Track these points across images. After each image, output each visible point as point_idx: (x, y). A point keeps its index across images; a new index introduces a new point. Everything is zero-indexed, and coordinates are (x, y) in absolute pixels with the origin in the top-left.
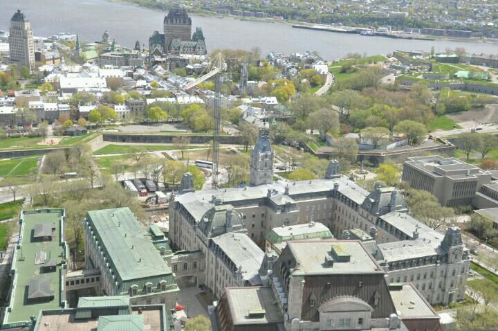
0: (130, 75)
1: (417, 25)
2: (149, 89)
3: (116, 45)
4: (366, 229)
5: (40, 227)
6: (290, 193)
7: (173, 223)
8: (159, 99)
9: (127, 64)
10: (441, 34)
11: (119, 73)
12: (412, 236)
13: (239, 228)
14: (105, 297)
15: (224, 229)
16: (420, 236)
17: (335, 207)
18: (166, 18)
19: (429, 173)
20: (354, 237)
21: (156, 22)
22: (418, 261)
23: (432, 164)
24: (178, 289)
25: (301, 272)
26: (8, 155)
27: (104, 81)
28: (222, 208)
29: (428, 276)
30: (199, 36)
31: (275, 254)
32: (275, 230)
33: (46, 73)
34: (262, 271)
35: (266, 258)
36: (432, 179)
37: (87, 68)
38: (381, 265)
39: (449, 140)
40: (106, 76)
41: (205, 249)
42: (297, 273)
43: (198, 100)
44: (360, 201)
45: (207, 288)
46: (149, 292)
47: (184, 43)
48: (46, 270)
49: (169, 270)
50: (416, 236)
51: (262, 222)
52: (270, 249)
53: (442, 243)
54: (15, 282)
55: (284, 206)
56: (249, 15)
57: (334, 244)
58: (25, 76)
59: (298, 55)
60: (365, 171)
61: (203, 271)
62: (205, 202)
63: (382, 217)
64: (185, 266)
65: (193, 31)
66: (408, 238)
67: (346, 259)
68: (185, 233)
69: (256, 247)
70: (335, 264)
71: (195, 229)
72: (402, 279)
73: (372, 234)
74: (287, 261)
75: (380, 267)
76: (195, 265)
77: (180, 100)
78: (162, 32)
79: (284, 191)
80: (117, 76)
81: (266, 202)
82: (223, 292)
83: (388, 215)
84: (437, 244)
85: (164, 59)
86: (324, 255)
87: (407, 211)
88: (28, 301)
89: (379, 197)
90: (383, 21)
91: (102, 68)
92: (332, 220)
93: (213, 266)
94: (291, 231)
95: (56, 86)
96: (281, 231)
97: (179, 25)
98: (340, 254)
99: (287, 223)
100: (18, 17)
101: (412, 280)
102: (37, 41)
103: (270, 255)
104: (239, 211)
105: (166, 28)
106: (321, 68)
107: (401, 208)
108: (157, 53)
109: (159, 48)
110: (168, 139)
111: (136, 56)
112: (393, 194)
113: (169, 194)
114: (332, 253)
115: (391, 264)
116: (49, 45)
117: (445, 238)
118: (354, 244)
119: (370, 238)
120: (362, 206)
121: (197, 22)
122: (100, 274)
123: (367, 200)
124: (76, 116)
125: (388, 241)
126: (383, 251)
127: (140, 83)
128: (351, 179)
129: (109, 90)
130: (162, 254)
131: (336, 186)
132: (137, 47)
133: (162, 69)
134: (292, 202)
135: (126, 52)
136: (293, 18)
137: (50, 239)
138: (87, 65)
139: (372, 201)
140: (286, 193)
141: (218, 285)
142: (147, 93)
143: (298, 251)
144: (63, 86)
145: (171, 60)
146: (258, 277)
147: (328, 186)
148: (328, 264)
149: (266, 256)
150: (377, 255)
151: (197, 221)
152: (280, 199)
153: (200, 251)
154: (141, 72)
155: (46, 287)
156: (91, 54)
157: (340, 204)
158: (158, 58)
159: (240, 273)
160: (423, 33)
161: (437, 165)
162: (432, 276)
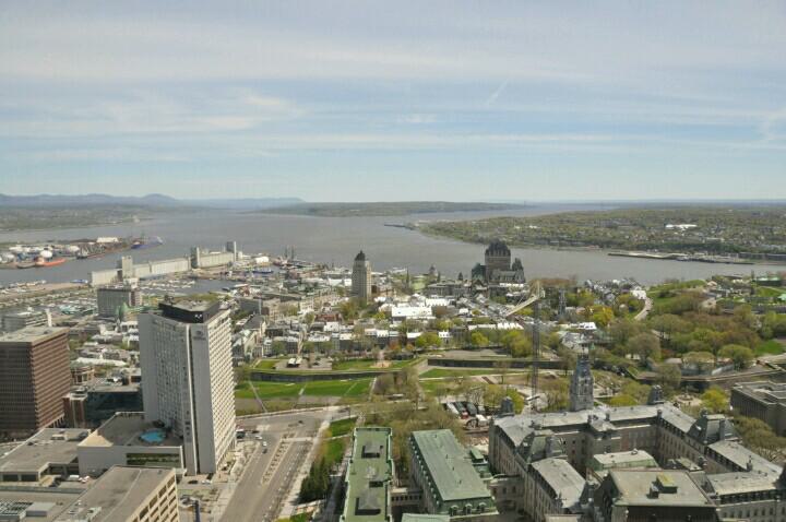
0: (454, 303)
1: (734, 251)
2: (471, 316)
3: (442, 277)
4: (693, 459)
5: (370, 444)
6: (612, 419)
8: (481, 326)
9: (451, 294)
10: (760, 257)
11: (443, 302)
12: (745, 467)
13: (559, 454)
14: (427, 515)
15: (543, 455)
16: (754, 468)
17: (658, 435)
18: (487, 251)
19: (760, 400)
20: (681, 467)
21: (478, 254)
22: (753, 496)
23: (763, 390)
24: (497, 513)
25: (624, 501)
26: (346, 376)
27: (430, 309)
28: (541, 433)
29: (767, 513)
30: (518, 266)
31: (597, 482)
32: (597, 457)
33: (380, 304)
34: (584, 498)
35: (587, 485)
36: (763, 407)
38: (712, 498)
39: (779, 365)
41: (524, 474)
42: (619, 503)
43: (518, 325)
44: (686, 428)
45: (526, 513)
46: (469, 513)
47: (504, 273)
48: (375, 484)
49: (488, 493)
50: (749, 468)
52: (591, 477)
53: (781, 476)
54: (348, 493)
55: (605, 432)
56: (565, 245)
57: (661, 474)
58: (362, 306)
59: (615, 281)
60: (689, 397)
61: (522, 496)
62: (525, 426)
63: (711, 446)
64: (504, 490)
65: (512, 261)
66: (741, 469)
67: (673, 490)
68: (504, 457)
69: (576, 473)
70: (661, 495)
71: (514, 453)
72: (736, 514)
73: (701, 464)
74: (608, 490)
75: (712, 500)
76: (514, 489)
77: (500, 326)
78: (483, 264)
79: (605, 417)
81: (586, 428)
82: (542, 518)
83: (717, 444)
84: (775, 478)
86: (649, 486)
87: (738, 441)
88: (359, 512)
89: (706, 424)
90: (699, 247)
92: (657, 448)
93: (532, 492)
94: (614, 459)
95: (388, 314)
96: (603, 458)
97: (496, 257)
98: (665, 484)
99: (609, 450)
100: (361, 257)
101: (748, 516)
102: (374, 276)
103: (591, 483)
104: (559, 437)
105: (487, 260)
106: (639, 293)
107: (729, 437)
108: (479, 283)
109: (481, 278)
110: (489, 364)
111: (460, 286)
112: (722, 422)
113: (489, 417)
114: (657, 483)
115: (723, 497)
116: (383, 279)
117: (784, 471)
118: (681, 474)
119: (699, 468)
120: (688, 434)
121: (516, 254)
122: (422, 492)
123: (693, 427)
124: (404, 341)
125: (718, 472)
126: (714, 484)
127: (463, 311)
128: (675, 405)
129: (434, 318)
130: (482, 476)
131: (660, 413)
132: (460, 277)
134: (614, 428)
135: (451, 283)
136: (608, 247)
137: (378, 456)
138: (416, 295)
139: (699, 428)
140: (607, 420)
141: (537, 510)
142: (469, 320)
143: (621, 479)
144: (394, 314)
145: (491, 289)
146: (578, 505)
147: (651, 412)
148: (653, 495)
149: (587, 485)
150: (707, 487)
152: (601, 426)
153: (518, 476)
154: (464, 300)
155: (374, 501)
156: (419, 286)
157: (664, 431)
158: (479, 288)
159: (560, 500)
160: (741, 257)
161: (768, 392)
162: (771, 513)
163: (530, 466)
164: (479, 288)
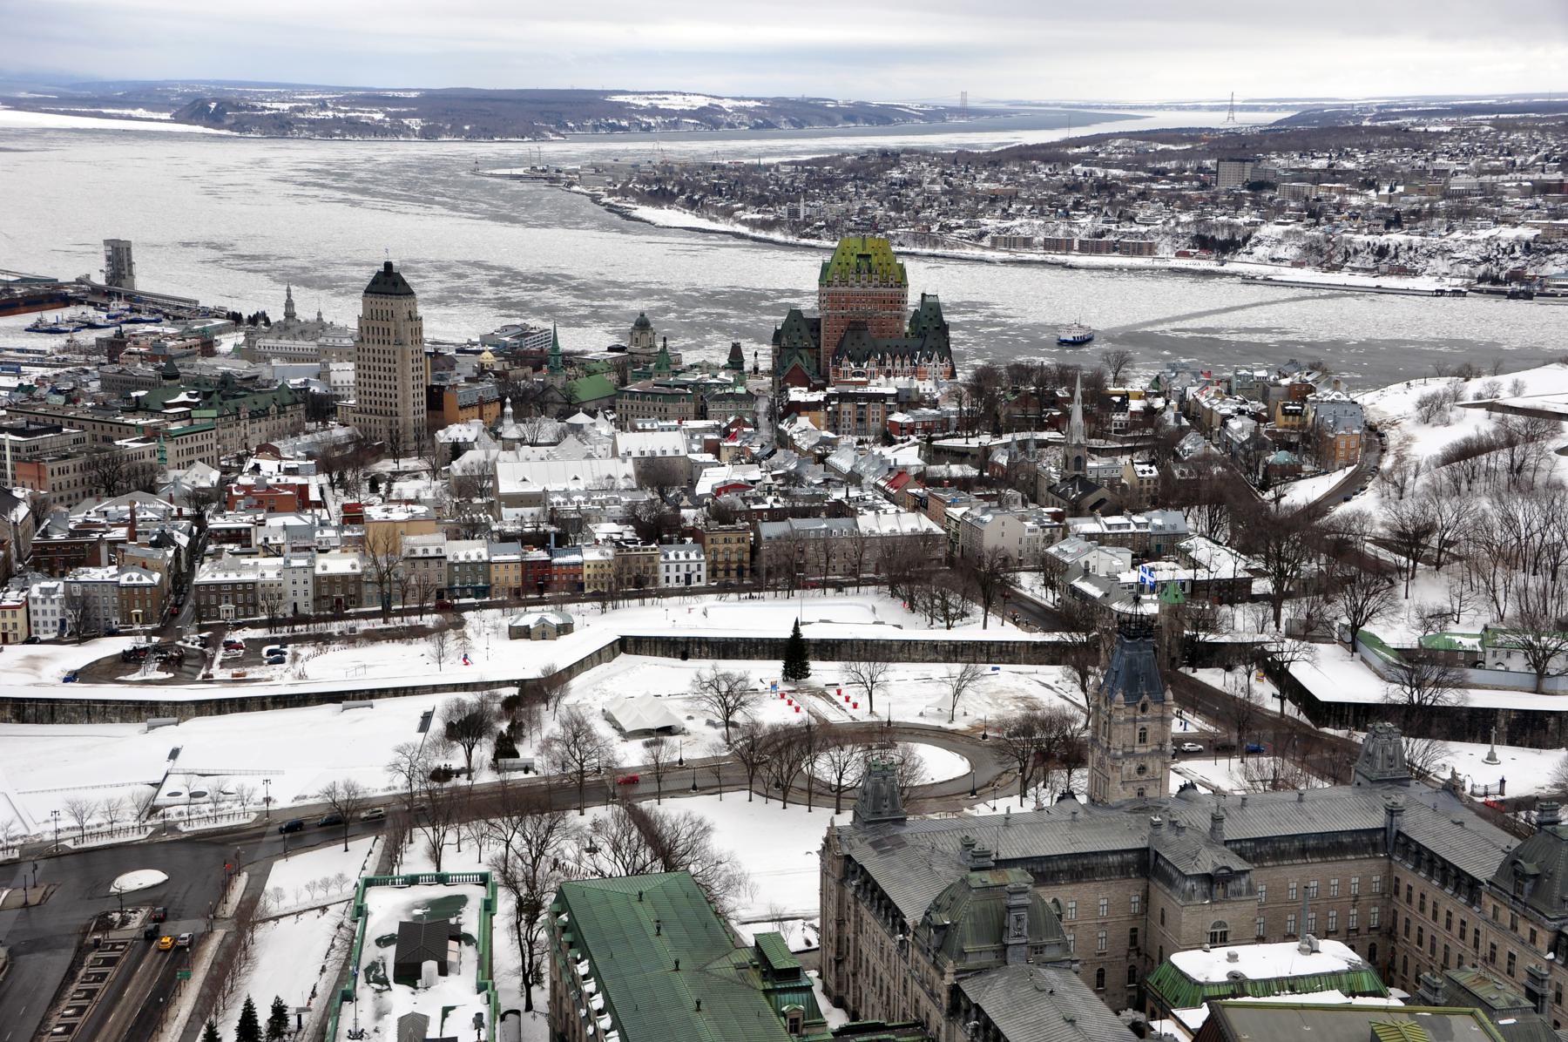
6: (1231, 831)
7: (832, 927)
9: (702, 414)
27: (629, 468)
37: (577, 428)
40: (636, 454)
51: (1134, 930)
80: (670, 453)
85: (819, 396)
91: (623, 429)
99: (1219, 938)
129: (648, 495)
133: (811, 426)
144: (507, 486)
151: (909, 921)
157: (1412, 878)
158: (797, 394)
163: (955, 991)
164: (797, 394)
